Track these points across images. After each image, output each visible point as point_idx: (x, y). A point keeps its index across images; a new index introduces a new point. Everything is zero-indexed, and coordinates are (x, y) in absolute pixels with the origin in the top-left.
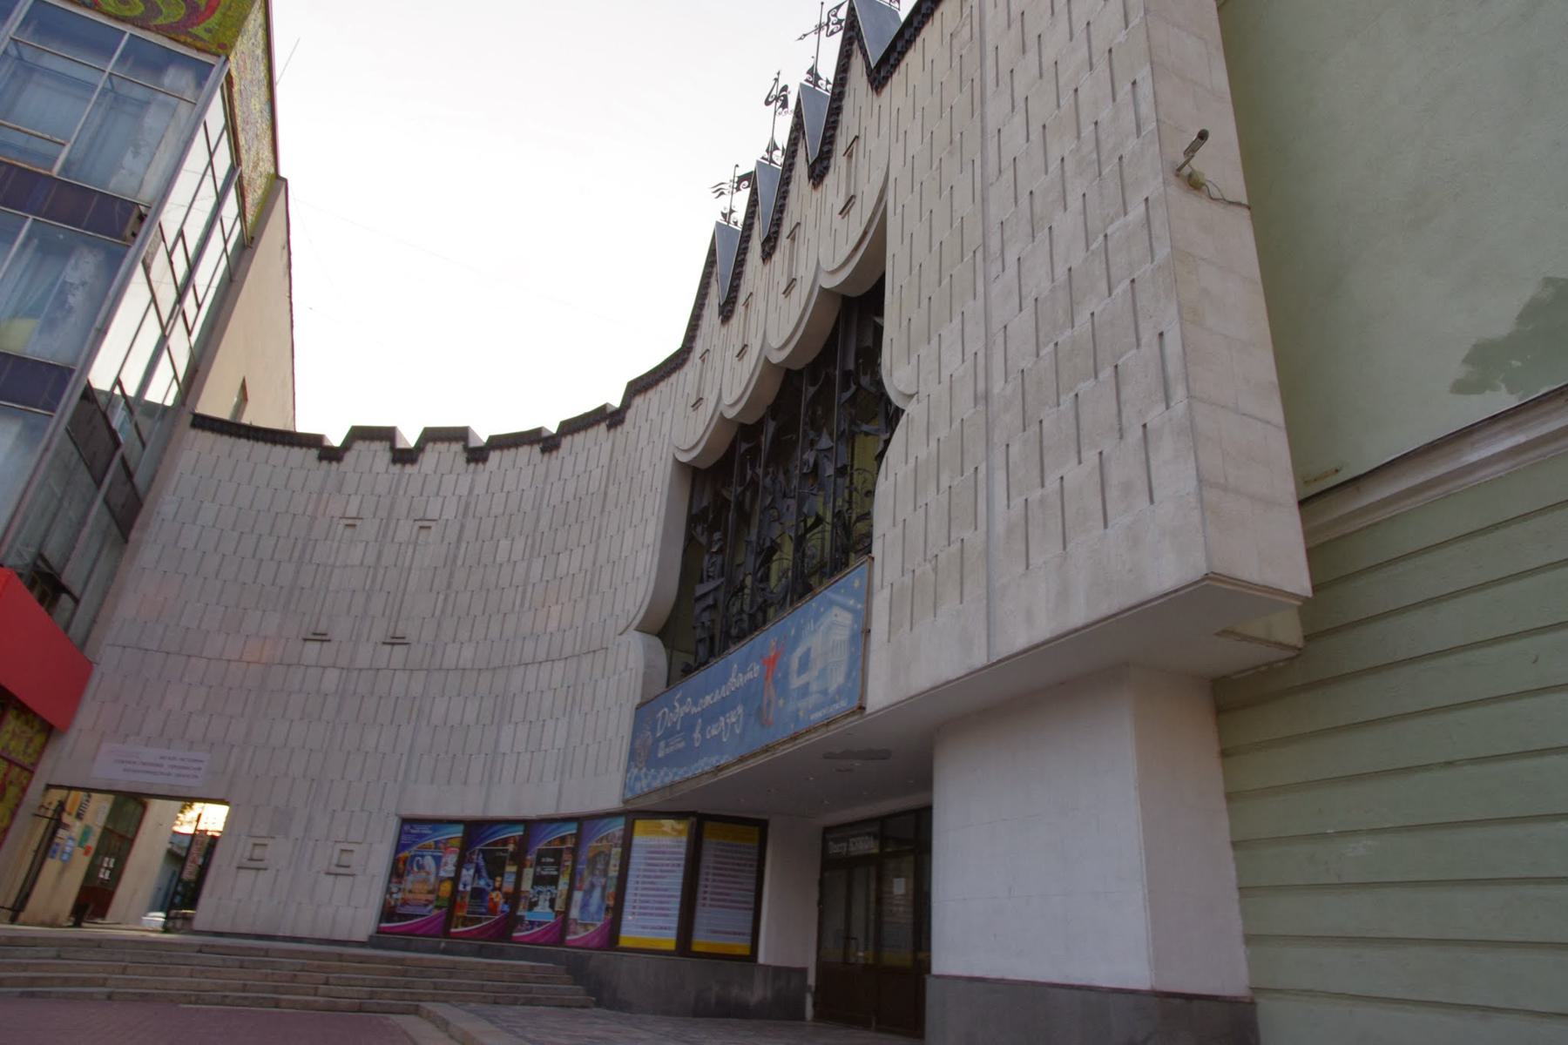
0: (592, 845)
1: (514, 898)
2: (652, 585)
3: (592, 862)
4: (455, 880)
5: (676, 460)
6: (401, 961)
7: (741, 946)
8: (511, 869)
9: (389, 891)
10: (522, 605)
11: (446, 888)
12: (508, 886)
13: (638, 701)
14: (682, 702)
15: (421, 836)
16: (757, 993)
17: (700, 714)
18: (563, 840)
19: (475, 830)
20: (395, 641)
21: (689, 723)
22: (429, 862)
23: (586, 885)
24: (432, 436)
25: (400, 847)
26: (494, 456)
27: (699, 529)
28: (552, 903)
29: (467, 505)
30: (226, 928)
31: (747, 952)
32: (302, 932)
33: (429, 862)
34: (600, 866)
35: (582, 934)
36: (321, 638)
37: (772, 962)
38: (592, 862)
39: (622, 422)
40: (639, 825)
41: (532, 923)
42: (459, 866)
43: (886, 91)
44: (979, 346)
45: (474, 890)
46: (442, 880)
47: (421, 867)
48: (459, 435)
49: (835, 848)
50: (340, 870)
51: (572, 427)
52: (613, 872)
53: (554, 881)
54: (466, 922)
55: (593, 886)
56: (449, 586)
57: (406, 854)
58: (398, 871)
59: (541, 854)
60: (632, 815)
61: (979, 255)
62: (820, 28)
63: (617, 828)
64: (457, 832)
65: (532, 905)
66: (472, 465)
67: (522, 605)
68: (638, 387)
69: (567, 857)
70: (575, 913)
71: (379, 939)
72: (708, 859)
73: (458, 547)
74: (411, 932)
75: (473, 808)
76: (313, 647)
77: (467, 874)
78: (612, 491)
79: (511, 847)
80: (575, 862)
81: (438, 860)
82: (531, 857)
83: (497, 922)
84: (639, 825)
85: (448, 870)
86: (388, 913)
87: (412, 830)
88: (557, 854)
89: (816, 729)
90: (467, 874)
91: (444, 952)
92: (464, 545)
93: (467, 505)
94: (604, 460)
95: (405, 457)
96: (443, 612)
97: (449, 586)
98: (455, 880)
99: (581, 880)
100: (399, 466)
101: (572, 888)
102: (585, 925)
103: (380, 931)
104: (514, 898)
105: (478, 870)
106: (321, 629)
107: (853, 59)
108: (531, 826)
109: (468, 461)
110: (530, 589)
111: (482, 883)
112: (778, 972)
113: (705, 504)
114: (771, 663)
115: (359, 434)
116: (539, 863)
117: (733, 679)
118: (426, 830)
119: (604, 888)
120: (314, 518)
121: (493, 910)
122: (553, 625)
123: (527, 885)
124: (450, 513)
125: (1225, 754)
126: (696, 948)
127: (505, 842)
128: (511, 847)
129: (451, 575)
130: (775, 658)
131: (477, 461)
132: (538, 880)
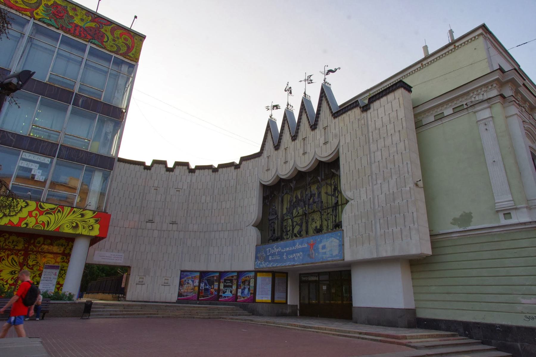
0: (243, 278)
1: (219, 290)
2: (257, 216)
3: (244, 282)
4: (199, 286)
5: (261, 183)
6: (206, 307)
7: (284, 301)
8: (216, 284)
9: (179, 289)
10: (212, 215)
11: (197, 288)
12: (216, 287)
13: (256, 244)
14: (277, 248)
15: (187, 275)
16: (289, 311)
17: (286, 252)
18: (232, 277)
19: (203, 274)
20: (173, 223)
21: (281, 254)
22: (190, 282)
23: (242, 287)
24: (177, 164)
25: (181, 278)
26: (197, 171)
27: (267, 201)
28: (231, 292)
30: (164, 301)
31: (285, 302)
32: (157, 300)
33: (190, 282)
34: (247, 283)
35: (243, 299)
36: (151, 221)
37: (291, 304)
38: (244, 282)
39: (239, 168)
40: (258, 274)
41: (225, 297)
42: (200, 283)
43: (337, 119)
44: (371, 196)
45: (205, 289)
46: (195, 286)
47: (188, 283)
48: (186, 164)
49: (304, 279)
50: (165, 284)
51: (221, 166)
52: (252, 284)
53: (231, 287)
54: (203, 297)
55: (244, 288)
56: (188, 208)
57: (183, 280)
58: (181, 284)
59: (225, 280)
60: (256, 272)
61: (370, 177)
62: (305, 80)
63: (252, 274)
64: (198, 274)
65: (224, 293)
66: (190, 174)
67: (212, 215)
68: (243, 159)
69: (235, 282)
70: (239, 294)
71: (179, 301)
72: (276, 281)
73: (189, 197)
74: (184, 299)
75: (203, 268)
76: (149, 225)
77: (202, 285)
78: (238, 187)
79: (215, 278)
80: (237, 282)
81: (193, 281)
82: (222, 280)
83: (212, 297)
84: (258, 274)
85: (197, 283)
86: (180, 295)
88: (231, 281)
89: (329, 262)
90: (202, 285)
91: (199, 304)
92: (191, 197)
94: (234, 177)
95: (169, 170)
97: (188, 208)
98: (199, 286)
99: (240, 286)
100: (168, 172)
101: (237, 289)
102: (244, 297)
103: (178, 299)
104: (219, 290)
106: (151, 219)
107: (323, 102)
108: (222, 274)
109: (189, 172)
110: (213, 211)
111: (207, 287)
112: (292, 306)
113: (267, 194)
114: (312, 246)
115: (155, 162)
116: (225, 282)
117: (297, 246)
118: (188, 274)
119: (249, 289)
120: (145, 186)
121: (212, 293)
122: (223, 221)
123: (222, 287)
124: (185, 187)
125: (411, 272)
126: (275, 301)
127: (213, 277)
128: (215, 278)
129: (188, 204)
130: (313, 244)
131: (192, 172)
132: (225, 286)
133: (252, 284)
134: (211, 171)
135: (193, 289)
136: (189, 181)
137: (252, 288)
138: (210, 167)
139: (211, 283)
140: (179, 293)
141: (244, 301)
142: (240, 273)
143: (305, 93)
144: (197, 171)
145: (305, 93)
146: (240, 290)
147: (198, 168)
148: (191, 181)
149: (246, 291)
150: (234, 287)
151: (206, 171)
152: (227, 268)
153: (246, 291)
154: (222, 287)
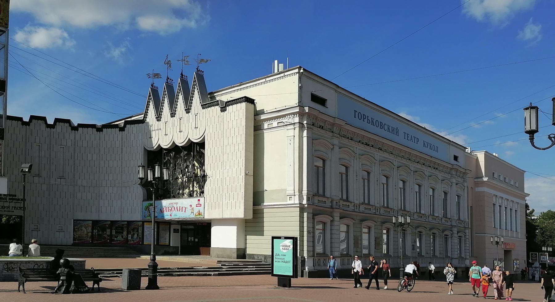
1: (111, 235)
3: (133, 230)
8: (108, 230)
11: (90, 234)
12: (108, 233)
23: (132, 233)
28: (122, 237)
29: (75, 142)
33: (83, 228)
38: (133, 230)
42: (93, 229)
47: (81, 230)
48: (68, 121)
55: (134, 234)
56: (74, 164)
64: (91, 222)
69: (125, 229)
70: (130, 238)
75: (95, 218)
85: (90, 229)
87: (77, 222)
88: (122, 228)
90: (95, 231)
93: (75, 142)
96: (74, 171)
98: (92, 232)
104: (111, 235)
105: (98, 230)
109: (72, 130)
118: (81, 222)
127: (106, 225)
129: (74, 161)
133: (140, 231)
134: (95, 130)
135: (87, 234)
136: (73, 139)
137: (140, 234)
138: (93, 126)
139: (104, 229)
140: (74, 237)
141: (134, 244)
142: (129, 223)
143: (182, 74)
144: (80, 129)
145: (182, 74)
146: (130, 236)
147: (80, 125)
148: (75, 138)
149: (136, 236)
150: (125, 233)
151: (90, 129)
152: (117, 218)
153: (136, 236)
154: (114, 232)
